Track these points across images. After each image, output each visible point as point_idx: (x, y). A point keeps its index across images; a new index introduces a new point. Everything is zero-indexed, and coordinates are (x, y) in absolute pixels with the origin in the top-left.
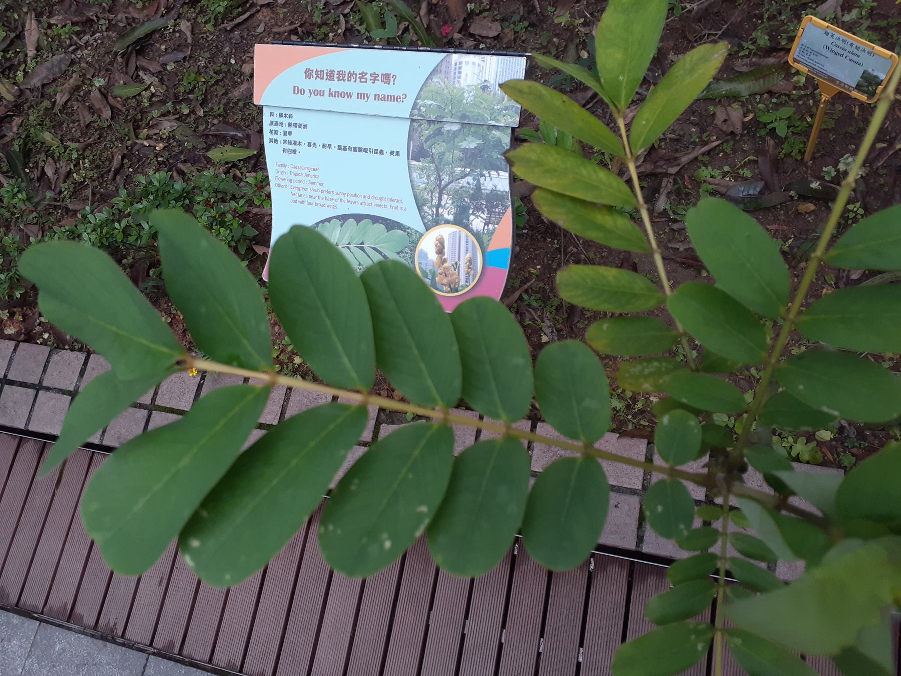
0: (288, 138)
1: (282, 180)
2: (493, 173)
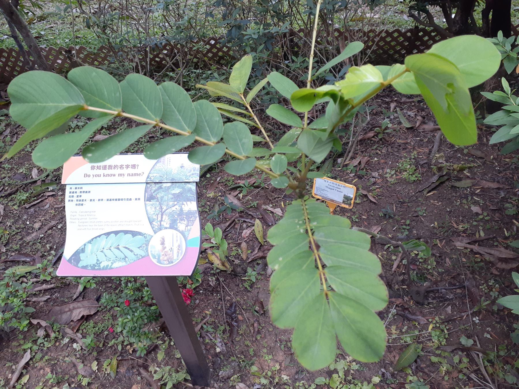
0: (79, 198)
2: (189, 203)
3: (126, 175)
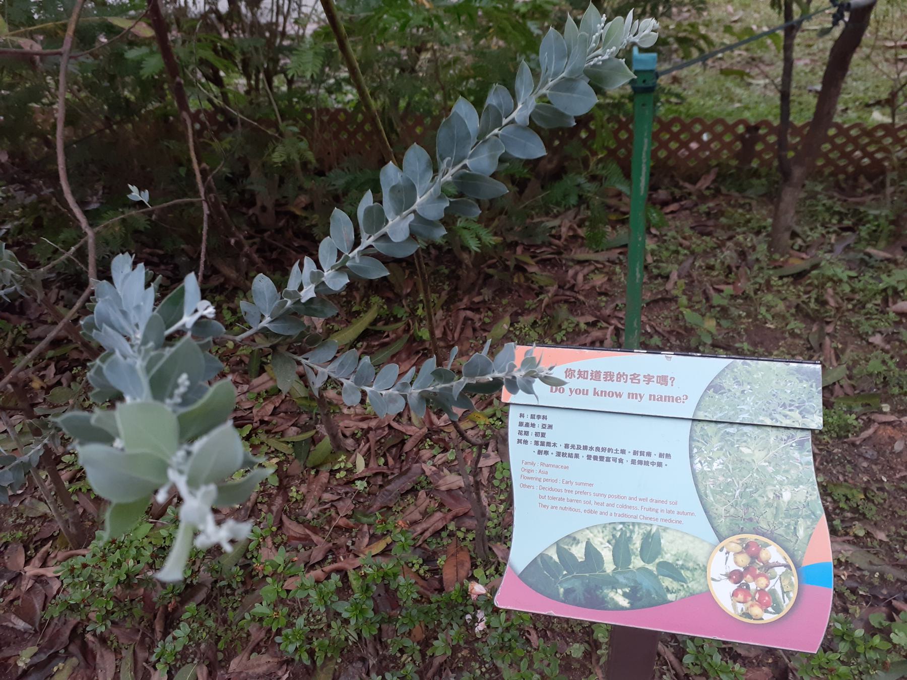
0: (540, 439)
1: (528, 478)
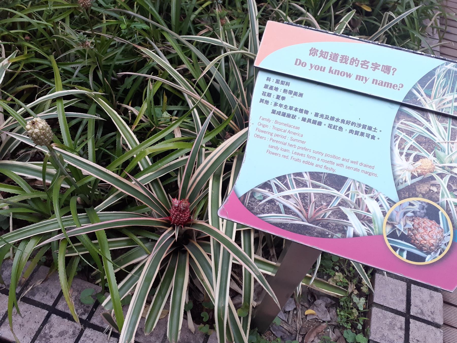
1: (262, 132)
3: (370, 81)
